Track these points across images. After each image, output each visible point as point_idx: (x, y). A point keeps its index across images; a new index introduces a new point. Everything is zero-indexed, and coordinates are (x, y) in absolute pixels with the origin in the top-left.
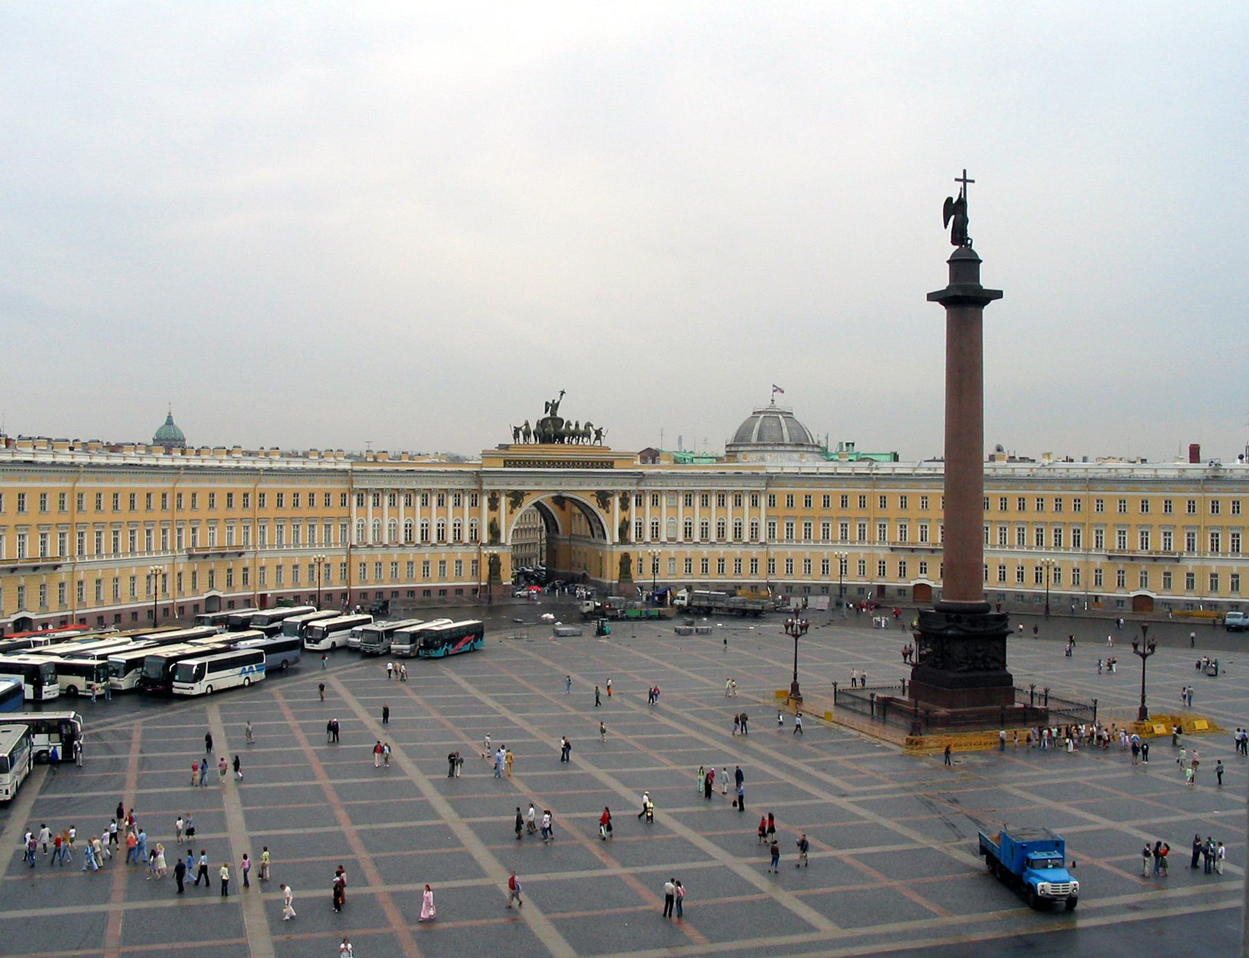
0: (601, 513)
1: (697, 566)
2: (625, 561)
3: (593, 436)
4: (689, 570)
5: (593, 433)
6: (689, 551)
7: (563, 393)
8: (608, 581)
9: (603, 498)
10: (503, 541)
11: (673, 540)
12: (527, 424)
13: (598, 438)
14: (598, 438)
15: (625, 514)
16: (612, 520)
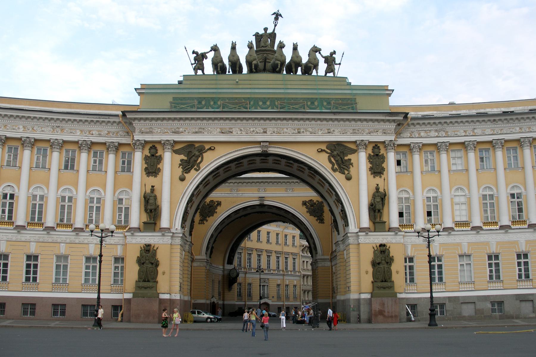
0: (336, 179)
1: (509, 267)
2: (382, 258)
3: (322, 67)
4: (495, 275)
5: (321, 61)
6: (493, 240)
7: (277, 16)
8: (353, 296)
9: (340, 154)
10: (164, 222)
11: (465, 224)
12: (215, 49)
13: (330, 69)
14: (330, 69)
15: (378, 180)
16: (355, 192)
